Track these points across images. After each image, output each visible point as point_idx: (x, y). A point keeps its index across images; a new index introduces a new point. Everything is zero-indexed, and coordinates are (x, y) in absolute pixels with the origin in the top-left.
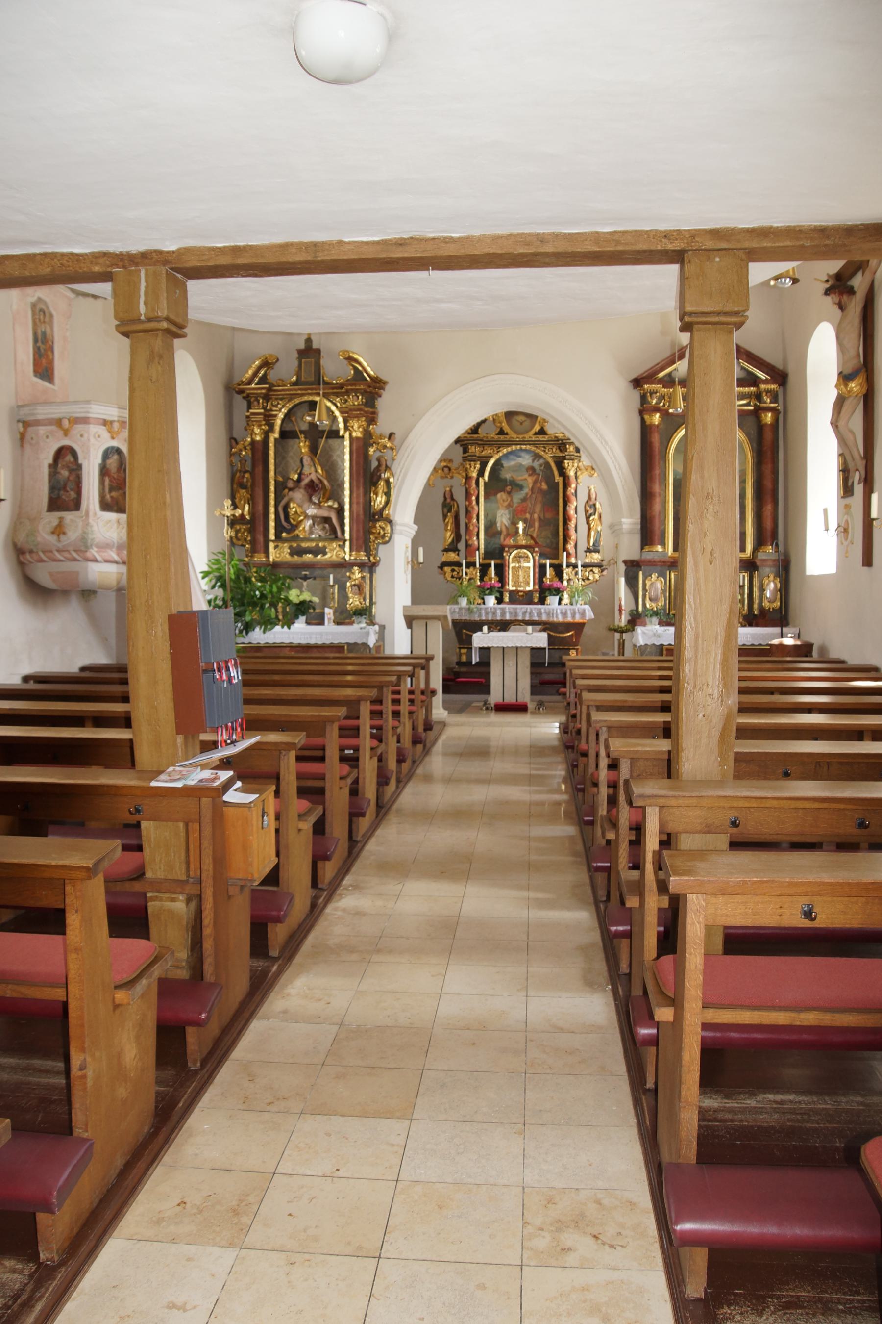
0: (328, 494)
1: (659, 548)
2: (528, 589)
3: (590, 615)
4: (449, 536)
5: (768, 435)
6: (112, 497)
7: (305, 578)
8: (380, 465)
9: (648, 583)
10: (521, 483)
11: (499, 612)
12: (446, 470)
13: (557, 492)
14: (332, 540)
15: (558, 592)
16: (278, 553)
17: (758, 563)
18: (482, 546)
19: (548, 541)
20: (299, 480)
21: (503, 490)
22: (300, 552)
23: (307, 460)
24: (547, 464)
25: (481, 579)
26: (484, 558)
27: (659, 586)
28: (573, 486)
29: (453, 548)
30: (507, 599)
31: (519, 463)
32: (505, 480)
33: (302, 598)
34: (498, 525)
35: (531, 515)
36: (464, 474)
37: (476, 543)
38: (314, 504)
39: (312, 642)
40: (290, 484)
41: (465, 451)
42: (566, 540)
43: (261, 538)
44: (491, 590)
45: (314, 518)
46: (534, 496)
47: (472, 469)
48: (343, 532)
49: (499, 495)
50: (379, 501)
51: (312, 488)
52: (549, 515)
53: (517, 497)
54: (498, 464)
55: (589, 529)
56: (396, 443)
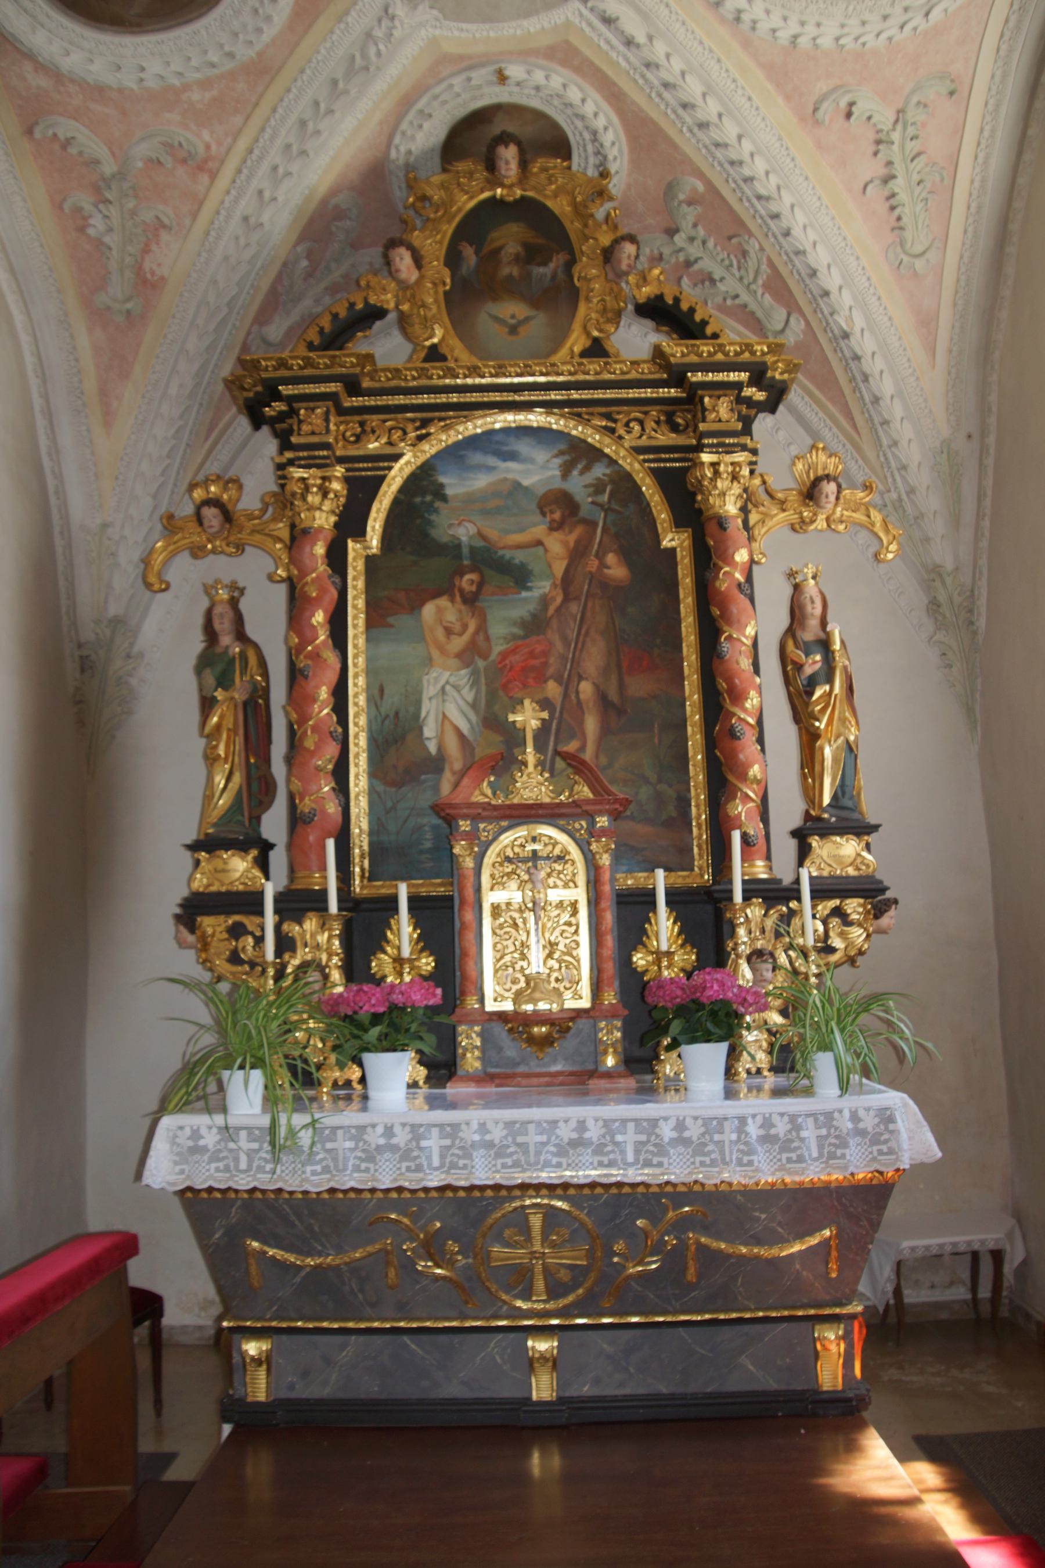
2: (570, 1004)
3: (915, 1140)
4: (226, 787)
10: (519, 557)
11: (433, 1143)
12: (211, 514)
13: (673, 585)
19: (645, 793)
21: (444, 589)
24: (624, 485)
25: (355, 968)
26: (372, 876)
28: (741, 556)
30: (471, 1062)
31: (511, 445)
32: (454, 549)
34: (429, 731)
35: (569, 683)
36: (282, 529)
37: (332, 808)
44: (391, 1028)
46: (574, 608)
47: (313, 499)
49: (429, 610)
52: (639, 686)
53: (504, 618)
54: (422, 484)
55: (810, 741)
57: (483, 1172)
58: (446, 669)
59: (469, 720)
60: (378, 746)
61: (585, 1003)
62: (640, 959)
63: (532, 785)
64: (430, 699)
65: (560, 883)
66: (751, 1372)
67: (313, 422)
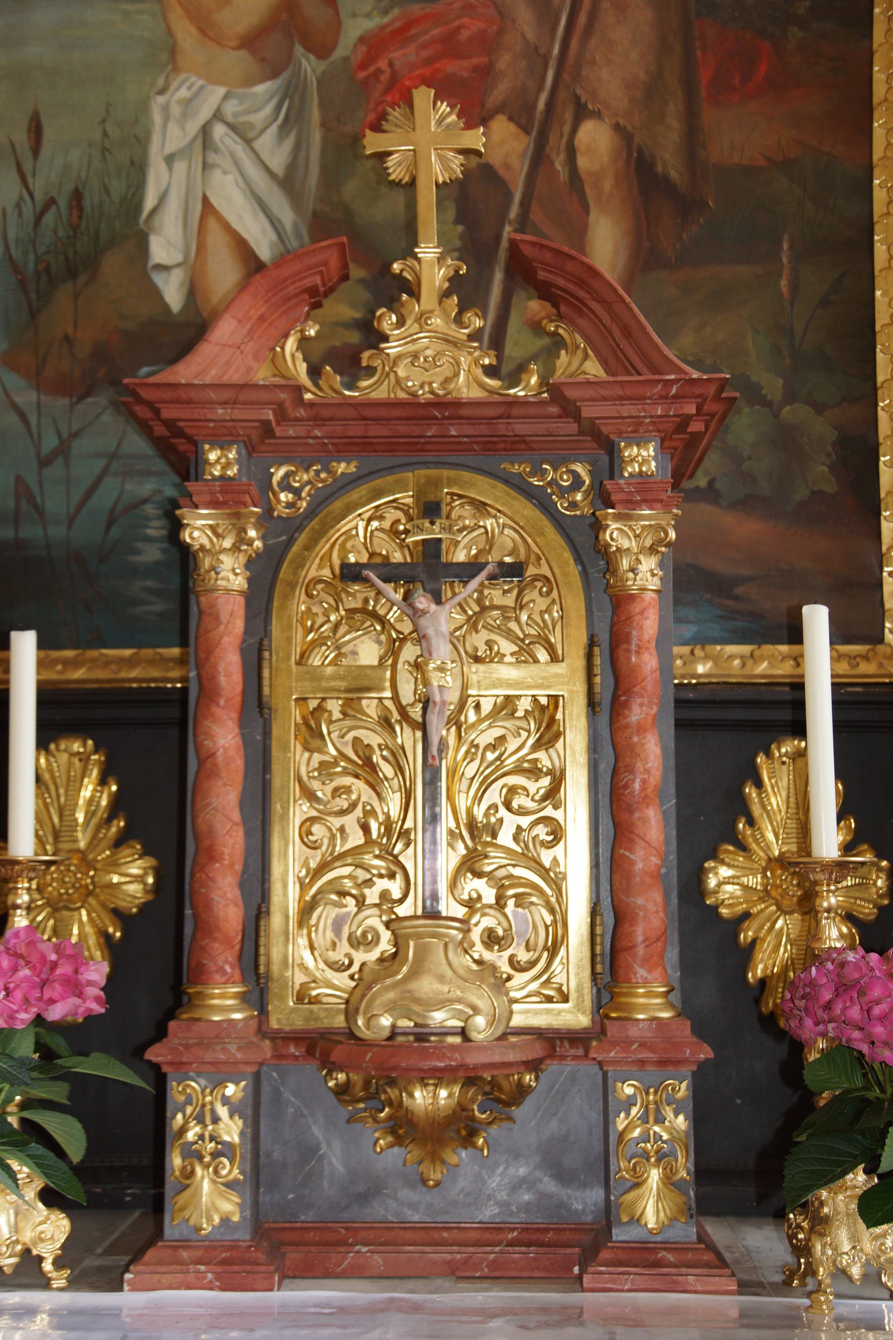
34: (165, 248)
52: (742, 135)
58: (214, 80)
59: (274, 222)
60: (22, 284)
61: (574, 1016)
62: (727, 882)
63: (430, 351)
64: (170, 160)
65: (506, 647)
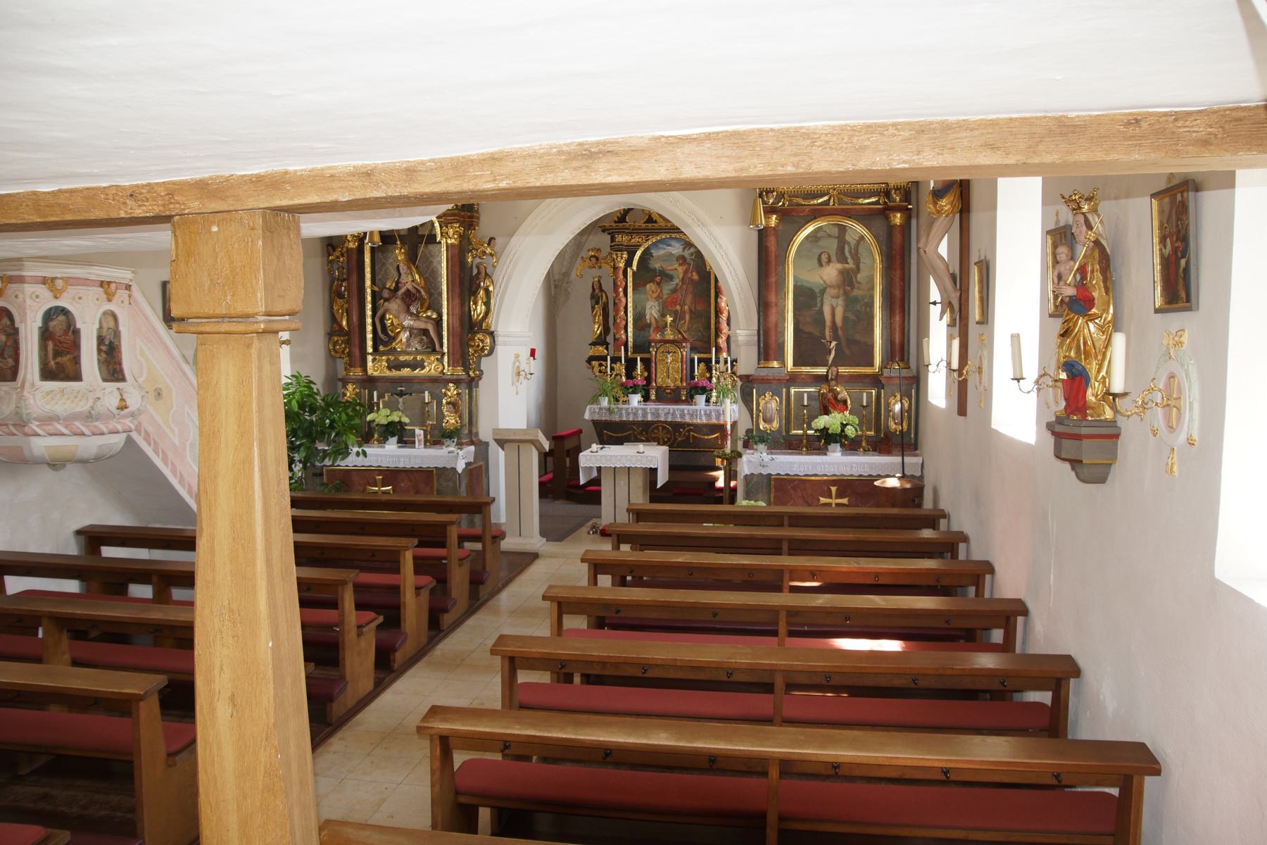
0: (426, 305)
1: (775, 364)
4: (597, 329)
5: (898, 238)
6: (57, 363)
7: (401, 394)
8: (479, 273)
9: (762, 403)
14: (429, 354)
15: (704, 390)
16: (375, 367)
17: (884, 381)
18: (630, 339)
20: (397, 289)
21: (652, 281)
22: (399, 366)
23: (403, 268)
27: (773, 405)
29: (601, 341)
30: (653, 397)
33: (390, 419)
35: (682, 306)
38: (411, 314)
39: (401, 465)
40: (386, 294)
41: (613, 240)
42: (717, 336)
43: (357, 352)
45: (411, 329)
48: (442, 346)
50: (481, 308)
51: (409, 298)
52: (700, 307)
53: (667, 289)
54: (647, 253)
56: (496, 248)
57: (649, 418)
66: (703, 461)
67: (619, 238)
